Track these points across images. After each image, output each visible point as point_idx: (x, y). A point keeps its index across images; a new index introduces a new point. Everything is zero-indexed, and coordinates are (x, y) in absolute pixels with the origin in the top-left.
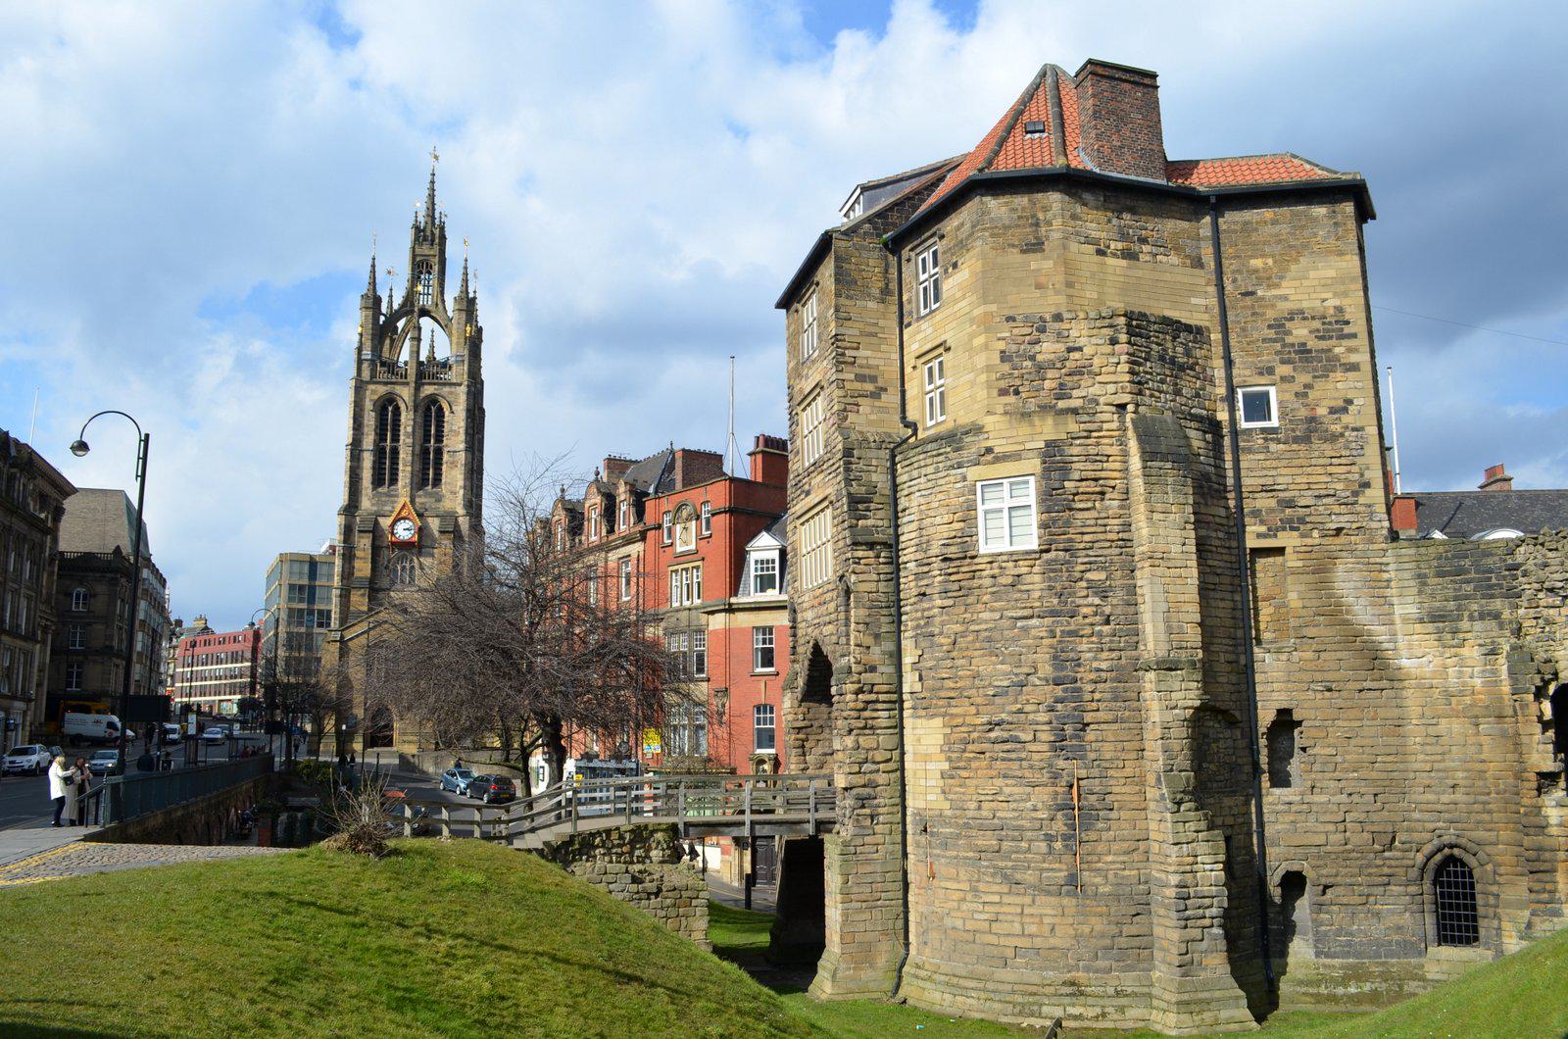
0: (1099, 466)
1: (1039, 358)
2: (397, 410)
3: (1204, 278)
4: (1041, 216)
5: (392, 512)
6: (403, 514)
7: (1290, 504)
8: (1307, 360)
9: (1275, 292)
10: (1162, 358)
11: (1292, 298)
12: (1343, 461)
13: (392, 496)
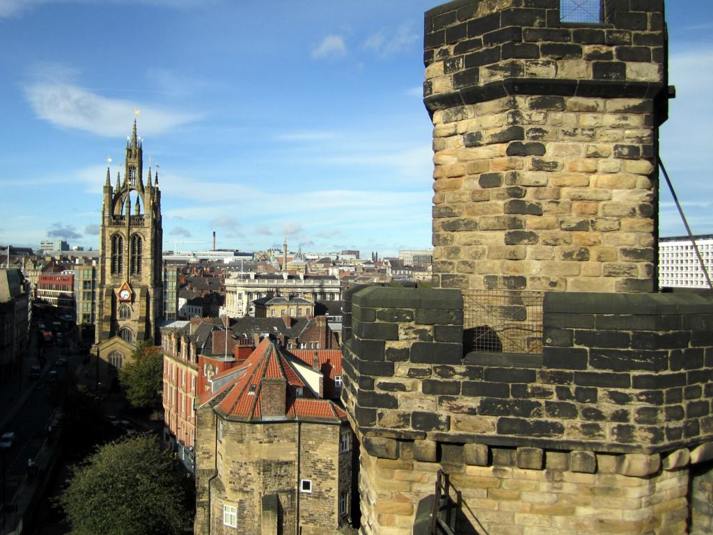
2: (121, 238)
3: (294, 446)
7: (312, 515)
10: (275, 476)
13: (119, 278)
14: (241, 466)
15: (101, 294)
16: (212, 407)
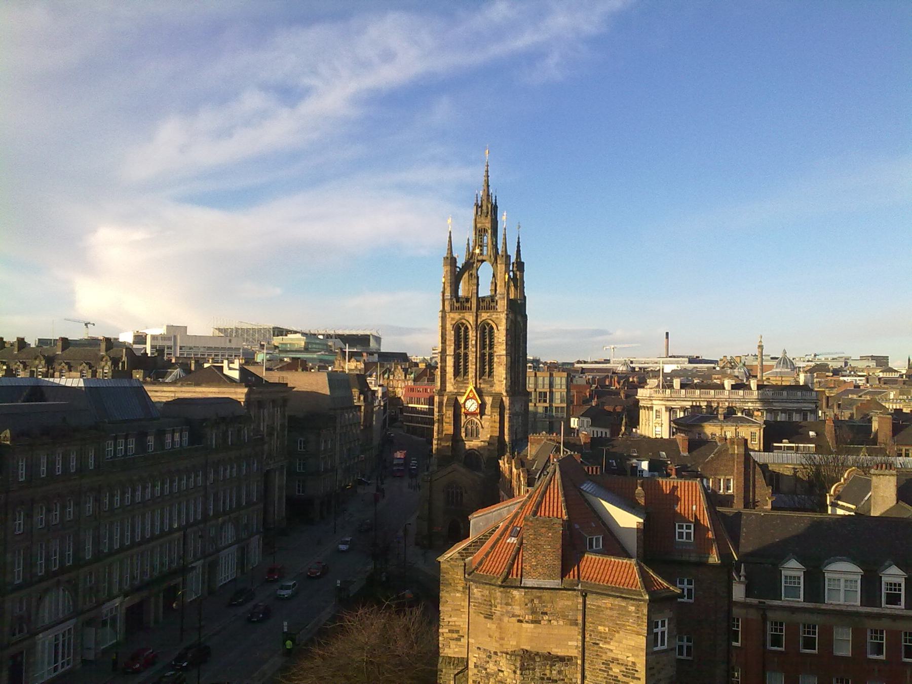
2: (467, 328)
3: (576, 631)
4: (493, 602)
5: (465, 393)
6: (471, 396)
11: (614, 651)
13: (465, 382)
14: (490, 657)
15: (441, 403)
16: (464, 560)
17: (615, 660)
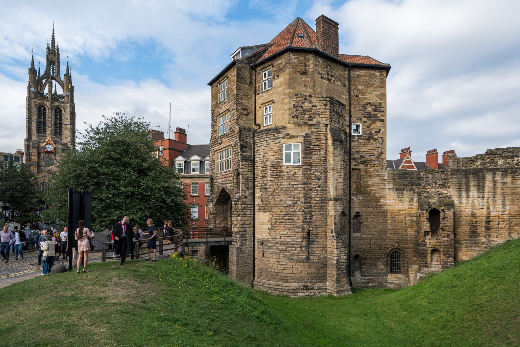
0: (320, 142)
1: (304, 108)
3: (345, 90)
6: (49, 142)
7: (363, 157)
8: (371, 117)
9: (364, 97)
11: (368, 99)
12: (377, 146)
17: (369, 104)
